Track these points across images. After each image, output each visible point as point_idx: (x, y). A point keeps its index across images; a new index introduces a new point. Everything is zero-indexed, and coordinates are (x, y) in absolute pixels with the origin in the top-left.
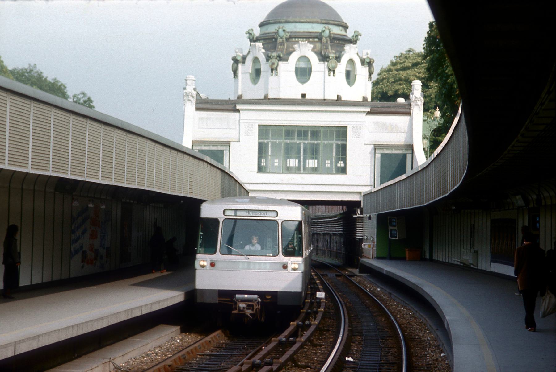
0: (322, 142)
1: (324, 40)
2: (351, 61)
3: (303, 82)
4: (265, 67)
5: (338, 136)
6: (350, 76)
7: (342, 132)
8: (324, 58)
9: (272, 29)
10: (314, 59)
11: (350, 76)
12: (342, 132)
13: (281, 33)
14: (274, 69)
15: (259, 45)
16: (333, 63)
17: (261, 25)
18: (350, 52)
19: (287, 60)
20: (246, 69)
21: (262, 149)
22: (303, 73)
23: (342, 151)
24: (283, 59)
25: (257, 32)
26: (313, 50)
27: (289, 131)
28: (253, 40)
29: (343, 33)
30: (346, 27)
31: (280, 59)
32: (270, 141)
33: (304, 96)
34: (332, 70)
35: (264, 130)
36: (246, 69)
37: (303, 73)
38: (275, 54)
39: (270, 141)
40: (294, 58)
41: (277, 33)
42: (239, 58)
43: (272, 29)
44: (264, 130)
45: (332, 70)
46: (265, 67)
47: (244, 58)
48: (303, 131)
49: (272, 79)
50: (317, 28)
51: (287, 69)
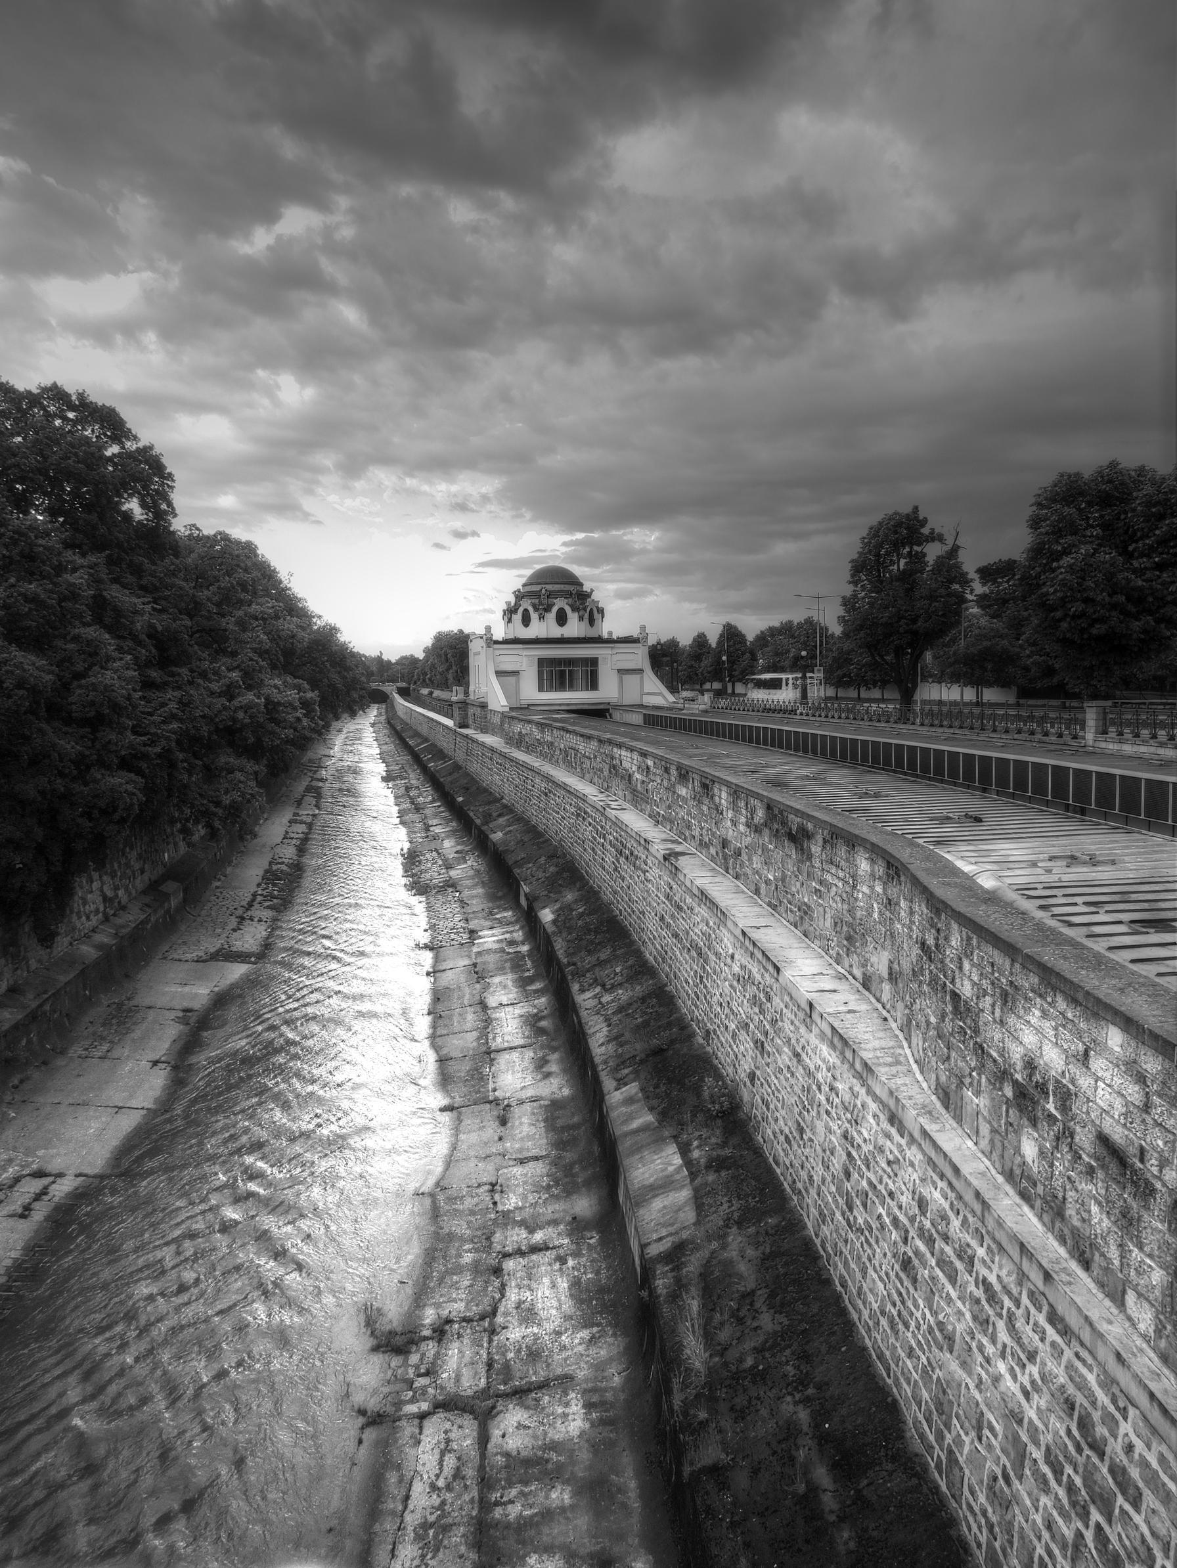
4: (534, 616)
6: (592, 622)
7: (593, 662)
8: (574, 609)
10: (568, 609)
12: (593, 662)
17: (524, 585)
20: (517, 618)
22: (562, 619)
24: (548, 609)
35: (542, 662)
36: (517, 618)
37: (562, 619)
40: (555, 609)
44: (542, 662)
45: (581, 618)
46: (534, 616)
51: (551, 616)
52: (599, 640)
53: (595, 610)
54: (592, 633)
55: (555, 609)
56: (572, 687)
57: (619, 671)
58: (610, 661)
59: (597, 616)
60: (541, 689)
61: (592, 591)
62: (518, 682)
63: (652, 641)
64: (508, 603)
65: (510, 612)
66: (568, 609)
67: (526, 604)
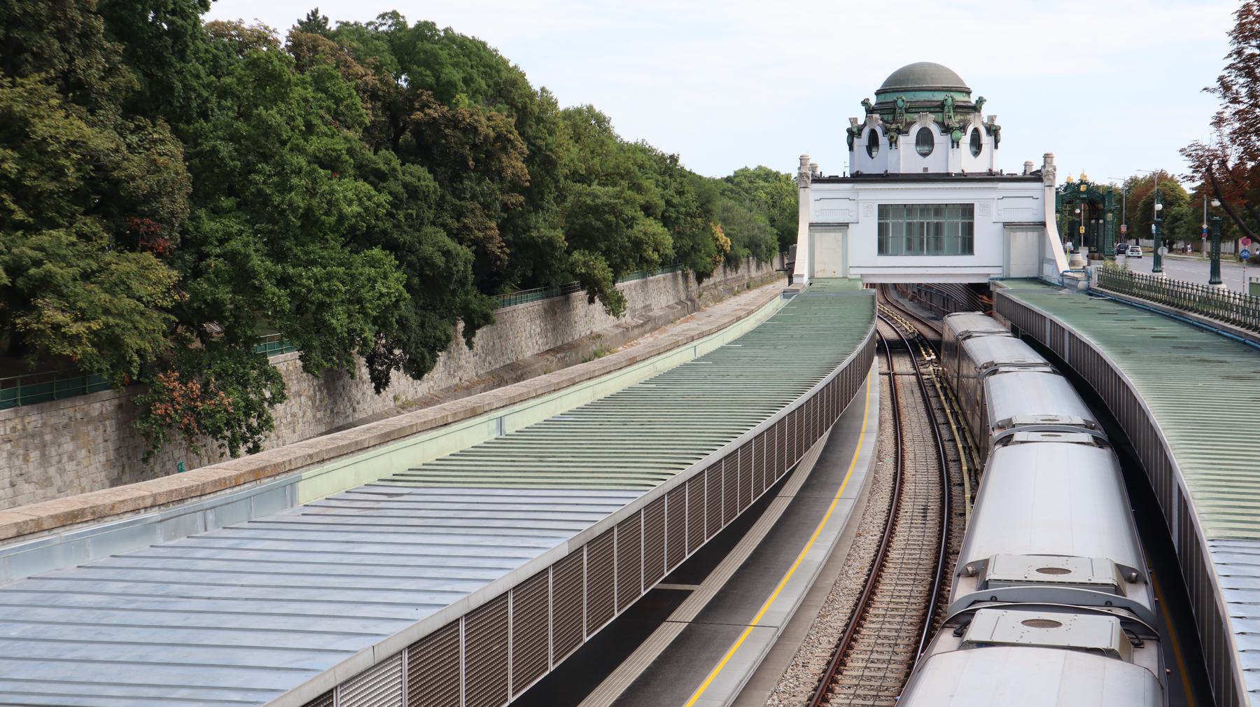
0: (945, 221)
1: (946, 109)
2: (976, 130)
3: (925, 155)
4: (883, 140)
5: (964, 216)
6: (976, 144)
7: (968, 210)
8: (946, 129)
9: (890, 98)
10: (935, 130)
11: (976, 144)
12: (968, 210)
13: (900, 103)
14: (893, 143)
15: (876, 116)
16: (957, 134)
17: (878, 93)
18: (976, 122)
19: (907, 133)
21: (882, 229)
23: (969, 229)
25: (873, 101)
26: (935, 121)
27: (909, 209)
28: (870, 111)
29: (966, 99)
30: (968, 93)
31: (899, 132)
32: (890, 221)
33: (926, 169)
34: (955, 143)
35: (884, 210)
38: (894, 126)
39: (890, 221)
40: (915, 130)
41: (895, 102)
42: (855, 130)
43: (890, 98)
44: (884, 210)
47: (861, 129)
48: (925, 209)
49: (892, 154)
50: (940, 97)
51: (907, 142)
52: (991, 177)
53: (983, 131)
54: (976, 165)
55: (915, 130)
56: (937, 249)
57: (1006, 225)
58: (992, 211)
59: (986, 140)
60: (882, 249)
61: (981, 101)
62: (845, 238)
63: (1060, 181)
64: (853, 121)
65: (853, 134)
66: (935, 130)
67: (877, 122)
